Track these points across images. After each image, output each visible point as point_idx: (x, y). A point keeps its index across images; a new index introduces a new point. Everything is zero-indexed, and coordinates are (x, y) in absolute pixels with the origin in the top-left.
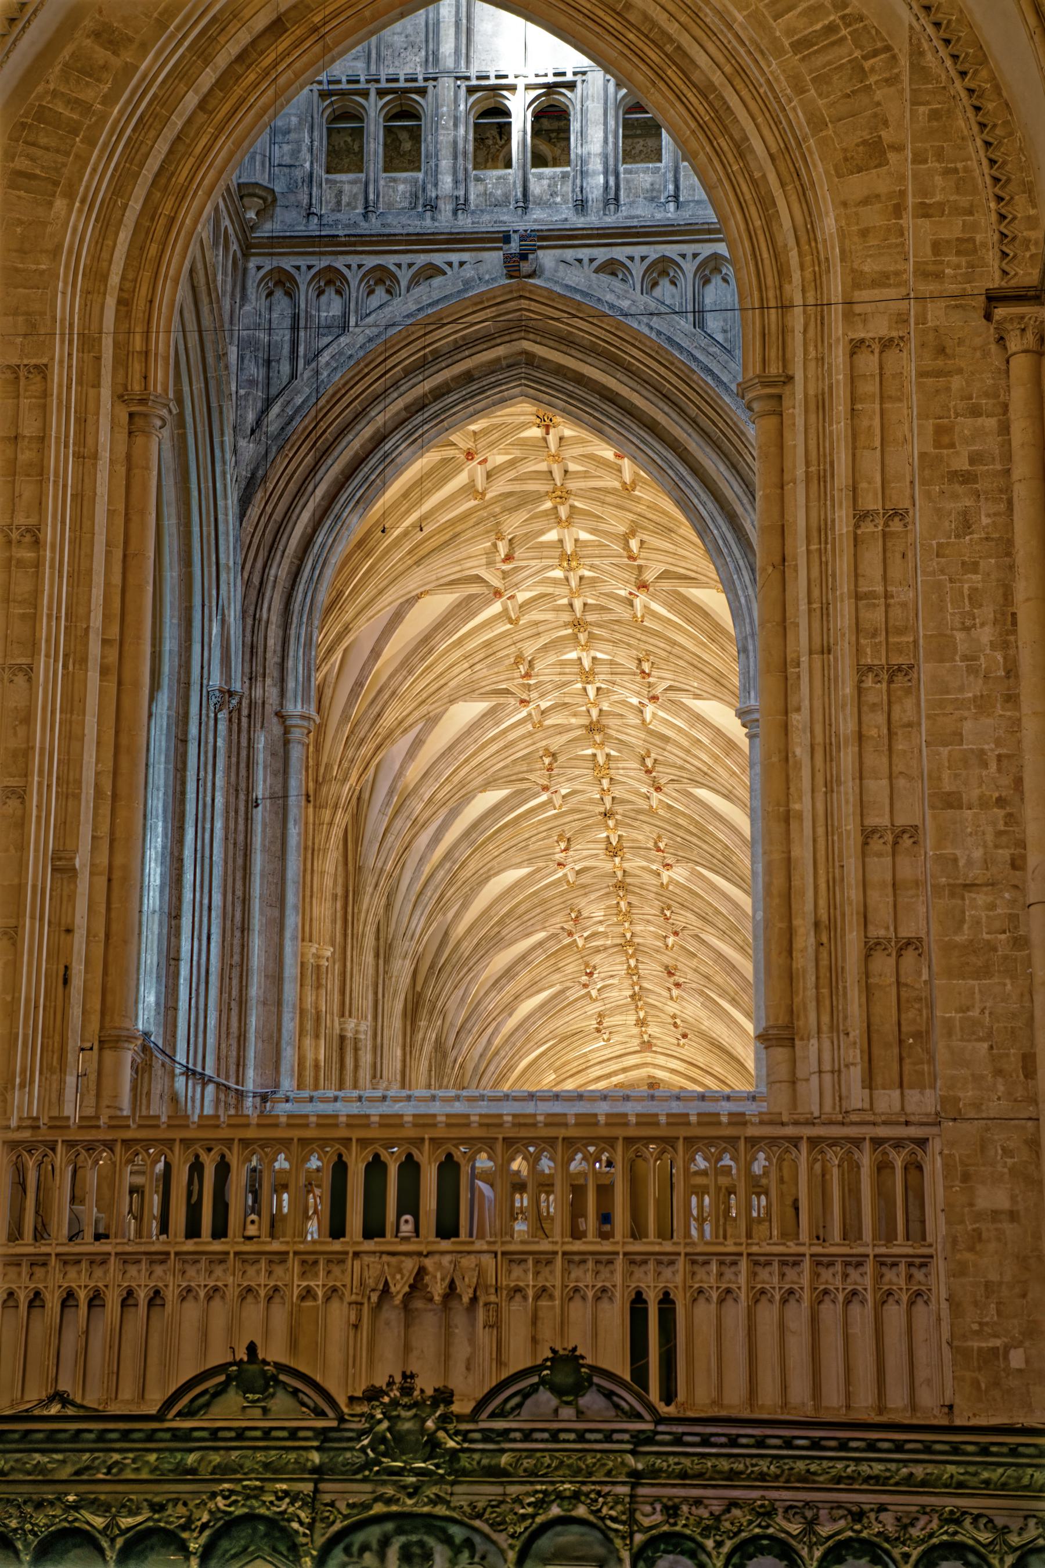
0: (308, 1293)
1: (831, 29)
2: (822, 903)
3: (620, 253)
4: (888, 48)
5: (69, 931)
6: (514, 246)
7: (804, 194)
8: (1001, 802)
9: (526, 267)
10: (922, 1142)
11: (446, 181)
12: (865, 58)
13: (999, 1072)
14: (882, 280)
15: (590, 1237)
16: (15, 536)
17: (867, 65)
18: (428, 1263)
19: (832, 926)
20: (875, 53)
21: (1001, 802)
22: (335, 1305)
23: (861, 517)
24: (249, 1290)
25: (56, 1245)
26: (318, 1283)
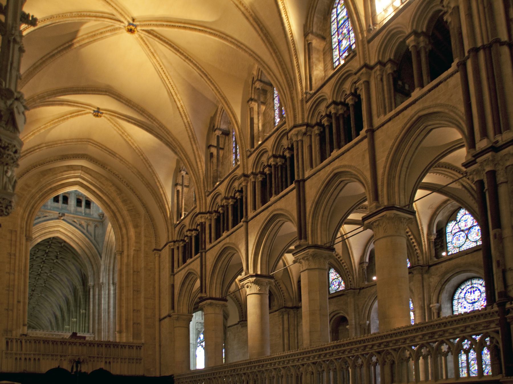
1: (131, 210)
7: (126, 229)
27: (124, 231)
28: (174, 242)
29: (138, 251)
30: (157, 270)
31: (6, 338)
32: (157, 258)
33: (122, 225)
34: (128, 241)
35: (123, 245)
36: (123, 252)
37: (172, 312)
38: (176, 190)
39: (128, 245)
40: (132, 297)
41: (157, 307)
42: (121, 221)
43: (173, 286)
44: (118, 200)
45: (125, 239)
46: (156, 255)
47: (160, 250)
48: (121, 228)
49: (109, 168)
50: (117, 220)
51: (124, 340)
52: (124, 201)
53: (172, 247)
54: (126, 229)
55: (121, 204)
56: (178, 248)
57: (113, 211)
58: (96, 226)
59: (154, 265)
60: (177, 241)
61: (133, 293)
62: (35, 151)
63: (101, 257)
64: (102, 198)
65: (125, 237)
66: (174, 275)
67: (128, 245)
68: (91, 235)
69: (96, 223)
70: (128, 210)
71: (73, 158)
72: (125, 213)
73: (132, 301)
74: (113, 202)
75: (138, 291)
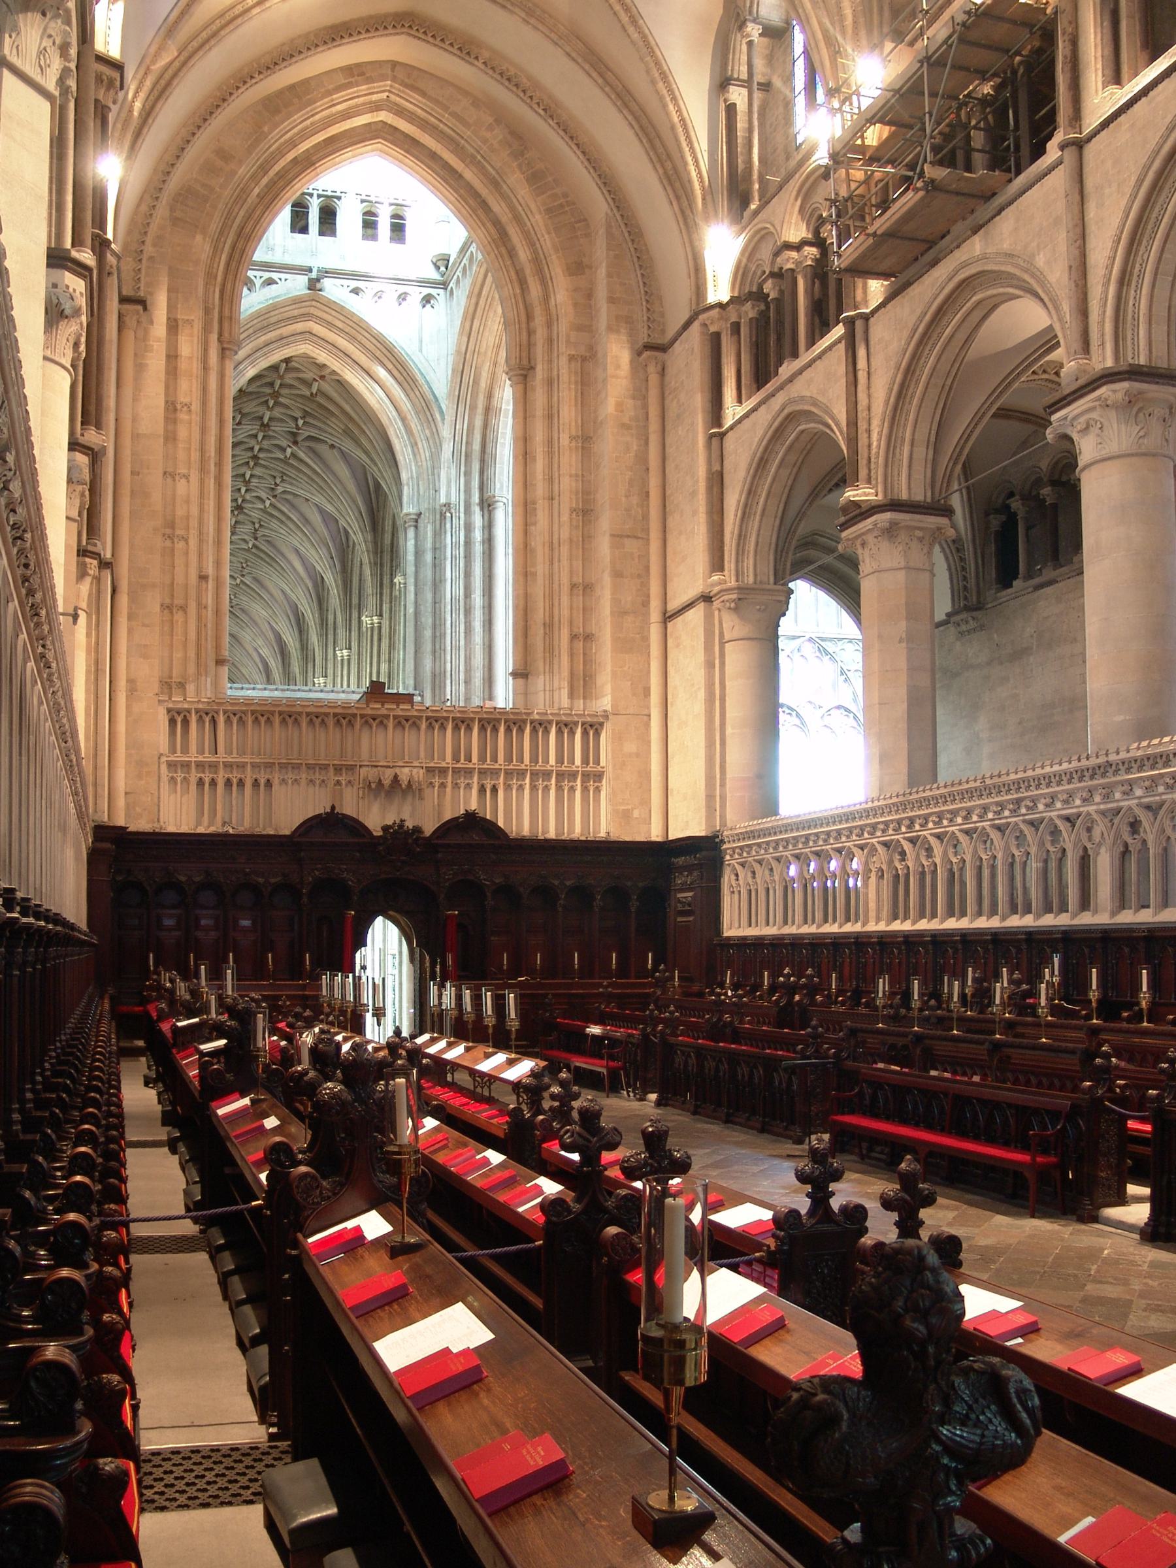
0: (338, 783)
1: (562, 206)
2: (547, 614)
4: (585, 220)
5: (205, 607)
7: (544, 282)
8: (639, 576)
10: (601, 724)
12: (576, 222)
13: (634, 694)
15: (462, 761)
16: (179, 407)
17: (577, 226)
18: (397, 770)
19: (551, 625)
20: (580, 221)
21: (639, 576)
22: (349, 789)
24: (311, 781)
25: (222, 757)
26: (343, 779)
29: (584, 359)
33: (528, 271)
34: (549, 324)
35: (530, 345)
39: (550, 341)
42: (523, 254)
44: (515, 180)
45: (539, 320)
50: (512, 253)
52: (536, 179)
54: (544, 282)
55: (523, 192)
57: (497, 223)
62: (249, 15)
65: (538, 312)
67: (550, 341)
70: (549, 211)
71: (368, 31)
72: (538, 220)
74: (495, 184)
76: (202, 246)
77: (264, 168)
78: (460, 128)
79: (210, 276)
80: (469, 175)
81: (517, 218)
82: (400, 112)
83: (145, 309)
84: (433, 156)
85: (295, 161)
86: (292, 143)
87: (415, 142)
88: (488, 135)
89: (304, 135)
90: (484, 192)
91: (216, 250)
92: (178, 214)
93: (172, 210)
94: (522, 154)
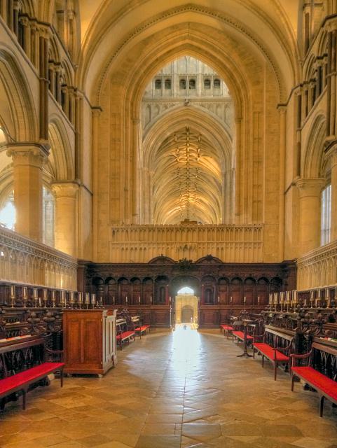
1: (251, 63)
3: (204, 103)
6: (187, 101)
9: (189, 104)
11: (175, 91)
14: (258, 103)
23: (254, 139)
27: (243, 93)
28: (301, 86)
30: (282, 131)
31: (112, 228)
32: (282, 116)
36: (242, 118)
37: (297, 177)
38: (304, 15)
40: (251, 170)
41: (281, 178)
42: (238, 81)
43: (299, 145)
46: (281, 112)
47: (286, 105)
48: (239, 90)
49: (219, 14)
50: (235, 81)
51: (243, 222)
52: (242, 55)
53: (298, 94)
56: (307, 93)
58: (226, 106)
59: (279, 125)
60: (305, 83)
61: (254, 165)
63: (232, 140)
64: (215, 58)
66: (301, 130)
68: (221, 118)
69: (226, 103)
70: (247, 65)
73: (251, 174)
75: (258, 162)
76: (123, 91)
77: (144, 63)
78: (214, 41)
79: (127, 99)
80: (218, 57)
81: (236, 69)
82: (193, 39)
83: (101, 110)
84: (207, 53)
85: (157, 60)
86: (155, 54)
87: (200, 49)
88: (223, 42)
89: (158, 51)
90: (224, 62)
91: (129, 91)
92: (115, 80)
93: (112, 79)
94: (237, 47)
